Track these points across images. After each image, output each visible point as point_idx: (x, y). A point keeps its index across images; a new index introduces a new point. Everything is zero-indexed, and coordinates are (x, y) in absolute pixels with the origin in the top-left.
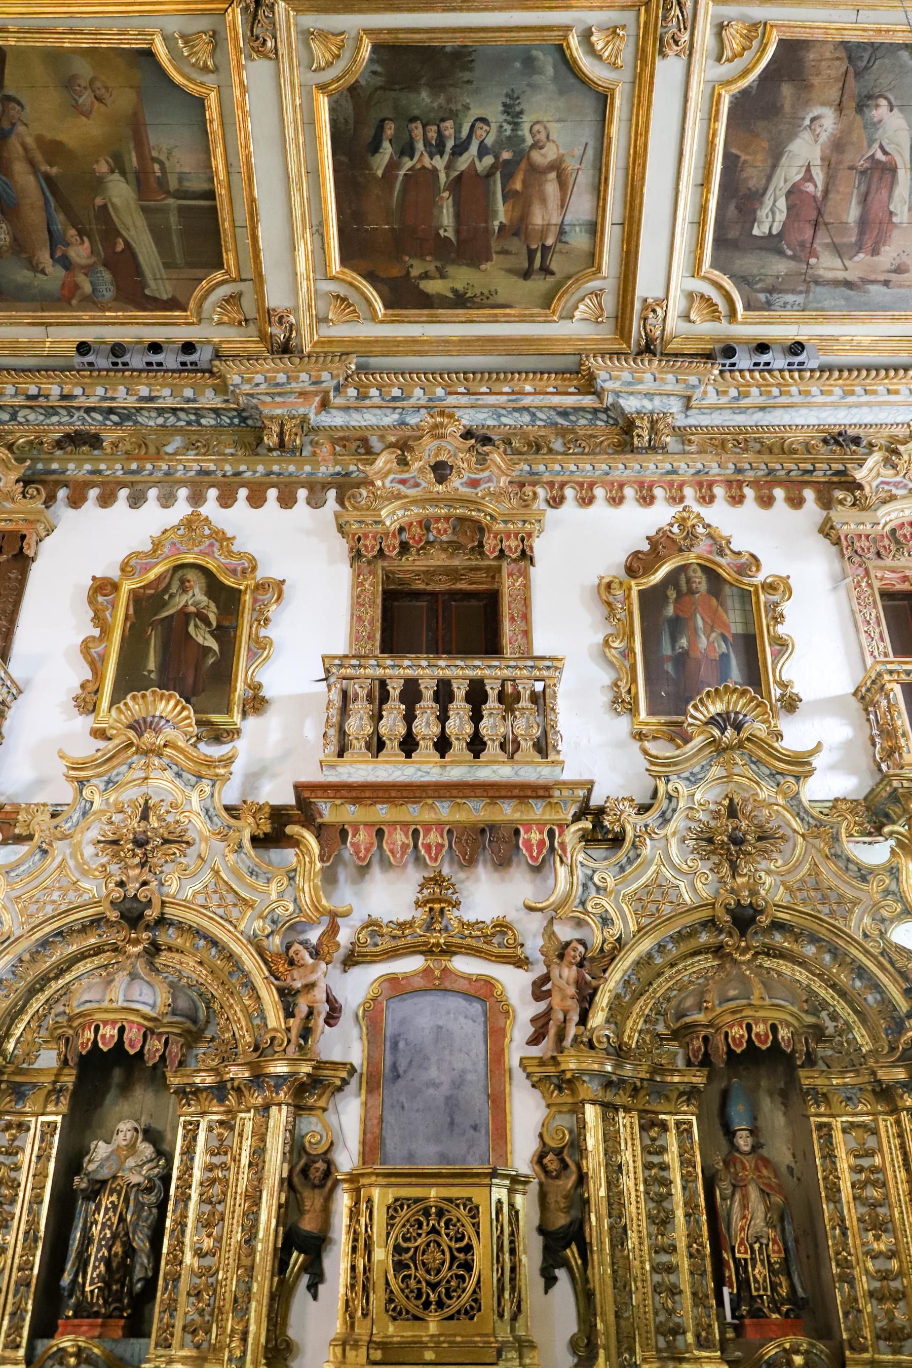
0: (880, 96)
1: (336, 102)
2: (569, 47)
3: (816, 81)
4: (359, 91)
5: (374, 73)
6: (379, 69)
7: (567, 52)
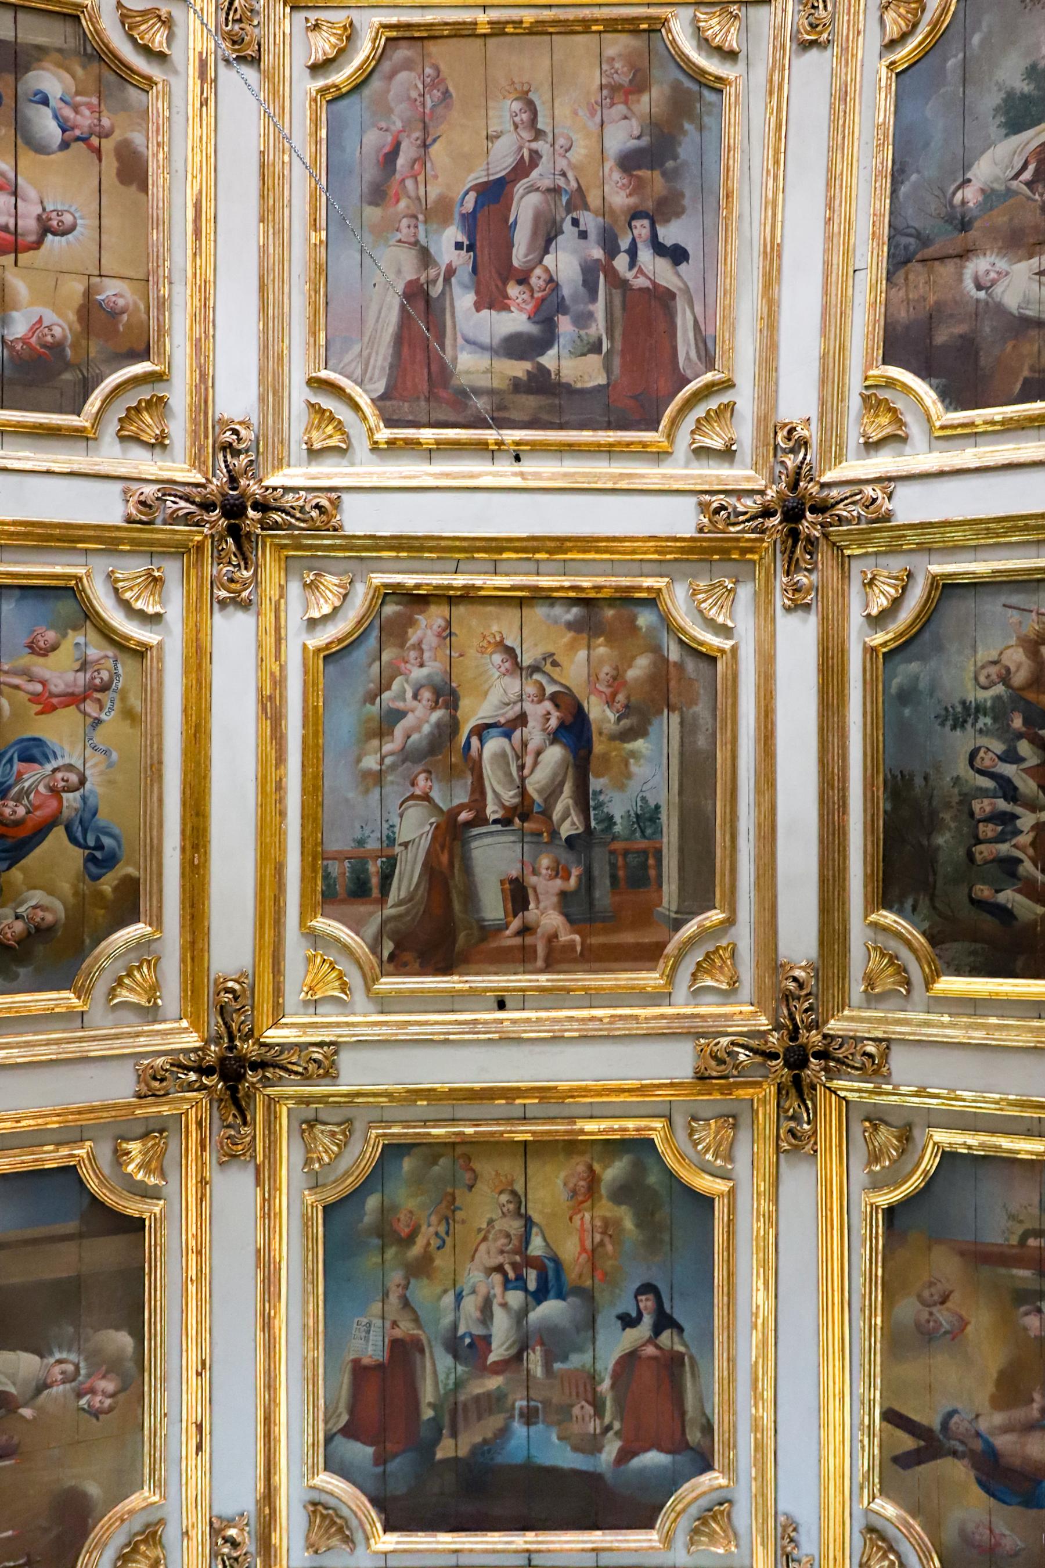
0: (951, 202)
1: (948, 964)
2: (884, 644)
3: (932, 299)
4: (935, 931)
5: (914, 909)
6: (909, 904)
7: (892, 645)
